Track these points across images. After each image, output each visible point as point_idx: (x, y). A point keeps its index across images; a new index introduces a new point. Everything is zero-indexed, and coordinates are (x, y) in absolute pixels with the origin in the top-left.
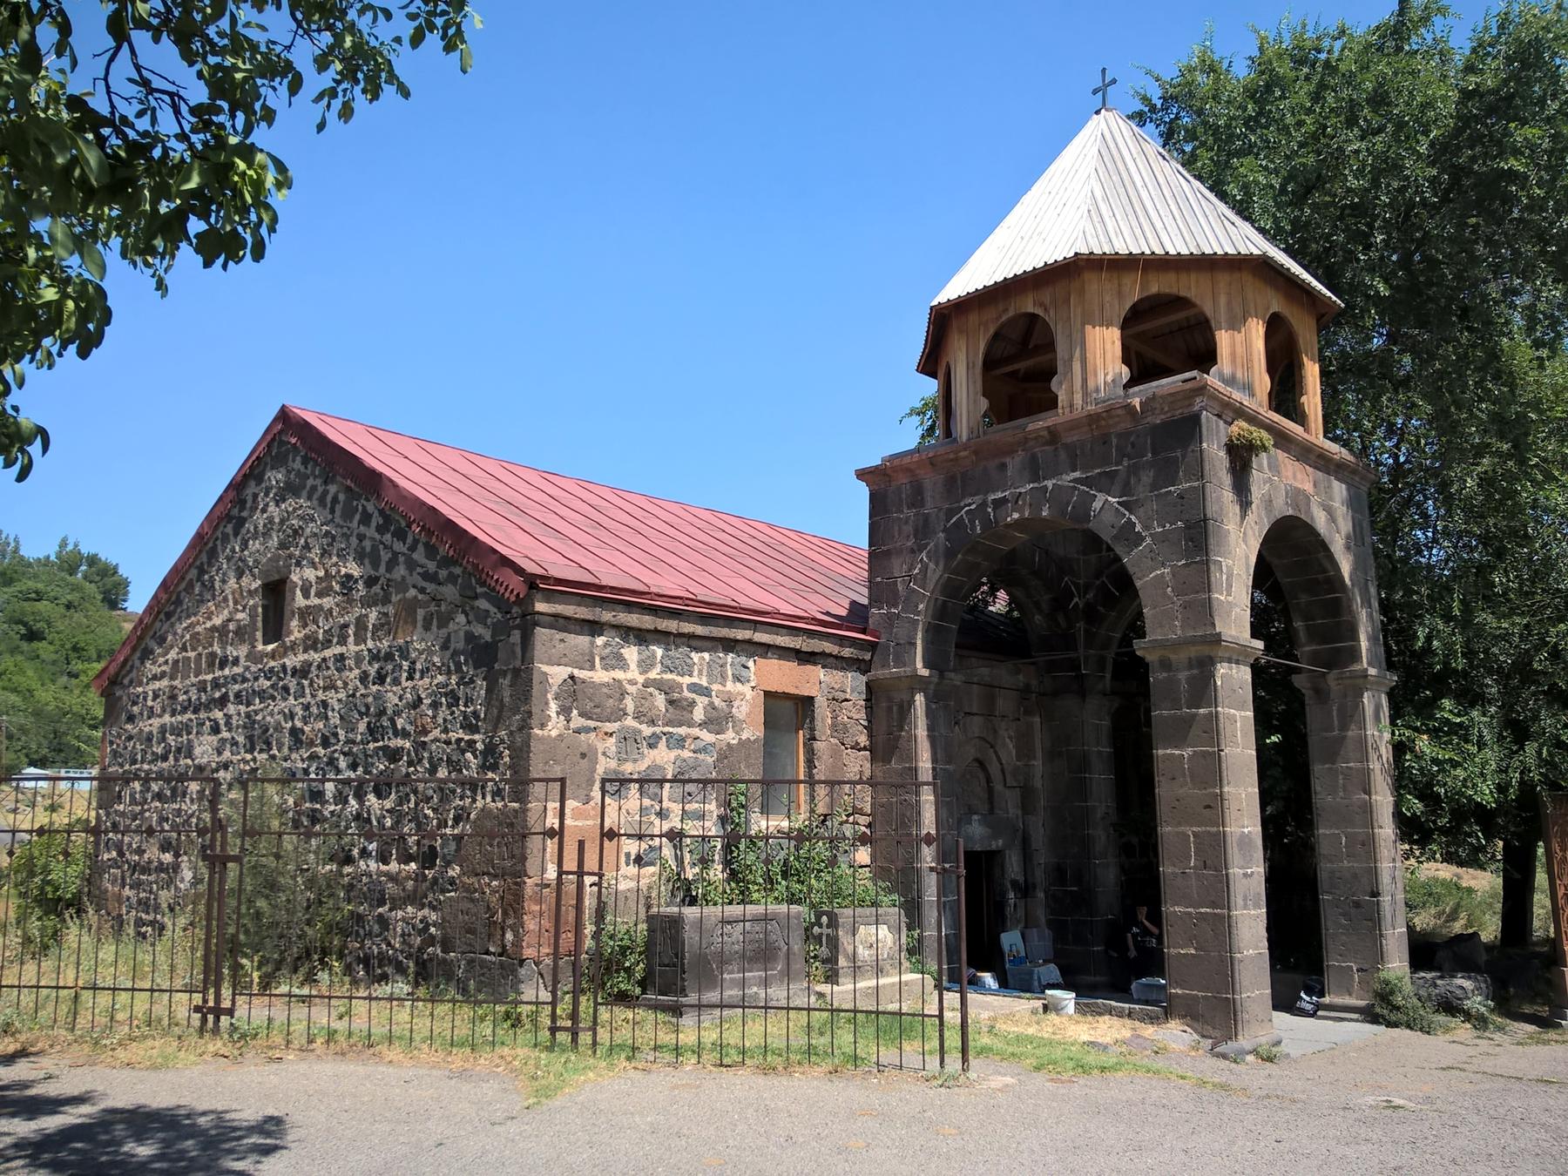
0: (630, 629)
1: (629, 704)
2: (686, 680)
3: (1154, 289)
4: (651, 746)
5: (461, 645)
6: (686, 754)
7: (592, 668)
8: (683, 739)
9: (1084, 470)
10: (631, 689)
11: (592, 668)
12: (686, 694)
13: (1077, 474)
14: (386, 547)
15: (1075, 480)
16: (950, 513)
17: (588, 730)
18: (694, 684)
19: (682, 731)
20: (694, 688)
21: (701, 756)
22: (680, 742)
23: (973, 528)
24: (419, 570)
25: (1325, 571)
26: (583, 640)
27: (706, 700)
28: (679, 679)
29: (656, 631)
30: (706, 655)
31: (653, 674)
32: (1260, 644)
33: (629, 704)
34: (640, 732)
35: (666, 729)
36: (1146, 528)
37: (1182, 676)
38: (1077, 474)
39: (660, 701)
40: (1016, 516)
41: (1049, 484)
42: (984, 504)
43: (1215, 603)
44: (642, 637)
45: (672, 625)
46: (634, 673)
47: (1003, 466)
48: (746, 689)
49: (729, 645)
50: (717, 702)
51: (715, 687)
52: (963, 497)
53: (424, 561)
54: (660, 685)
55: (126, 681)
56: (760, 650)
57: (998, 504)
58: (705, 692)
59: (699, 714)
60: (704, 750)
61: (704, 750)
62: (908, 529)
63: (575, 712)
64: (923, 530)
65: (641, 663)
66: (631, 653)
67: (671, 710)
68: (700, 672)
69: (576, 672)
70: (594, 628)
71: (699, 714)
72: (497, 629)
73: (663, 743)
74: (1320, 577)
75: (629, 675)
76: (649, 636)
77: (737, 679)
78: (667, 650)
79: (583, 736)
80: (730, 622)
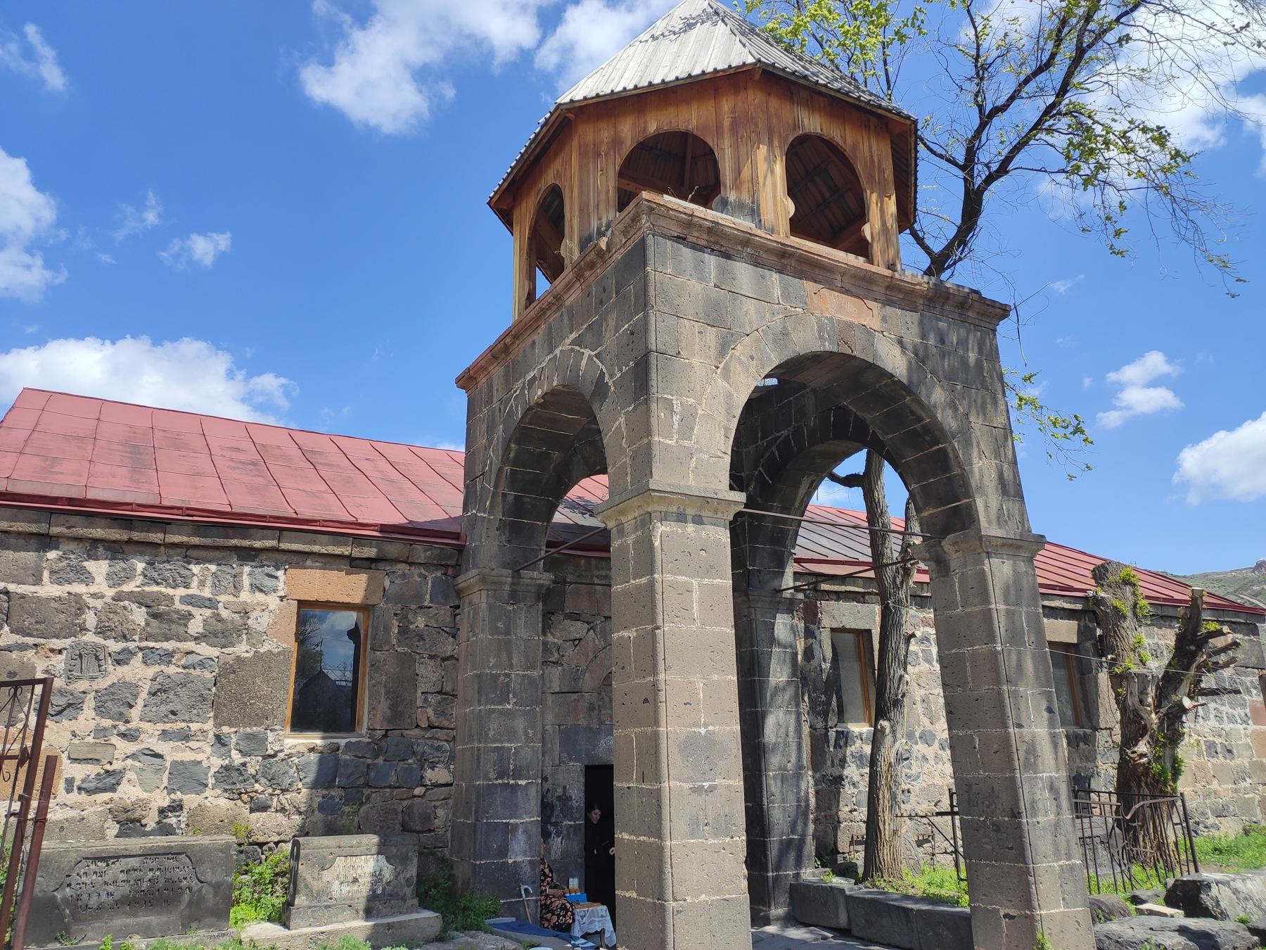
0: (95, 541)
1: (90, 619)
2: (181, 591)
3: (652, 128)
4: (119, 662)
6: (171, 670)
7: (38, 581)
8: (170, 654)
10: (92, 602)
11: (38, 581)
12: (178, 605)
13: (574, 335)
15: (574, 343)
17: (23, 647)
18: (192, 596)
19: (169, 645)
20: (190, 600)
21: (198, 672)
22: (167, 657)
25: (920, 419)
26: (28, 557)
27: (208, 612)
28: (170, 591)
29: (130, 542)
30: (213, 568)
31: (129, 587)
32: (741, 497)
33: (90, 619)
34: (104, 647)
35: (144, 644)
36: (611, 376)
37: (630, 540)
39: (139, 616)
40: (539, 392)
41: (557, 352)
42: (523, 388)
43: (656, 450)
44: (116, 550)
45: (157, 537)
46: (100, 585)
47: (534, 342)
48: (273, 601)
49: (248, 555)
50: (224, 614)
51: (223, 598)
54: (141, 600)
56: (294, 558)
58: (211, 604)
59: (195, 626)
60: (202, 665)
61: (202, 665)
62: (484, 427)
63: (6, 628)
64: (490, 430)
65: (109, 577)
66: (99, 568)
67: (155, 623)
68: (202, 584)
69: (12, 587)
70: (45, 542)
71: (195, 626)
73: (137, 660)
74: (918, 426)
75: (93, 589)
76: (126, 548)
77: (256, 588)
78: (151, 564)
79: (14, 655)
80: (243, 531)
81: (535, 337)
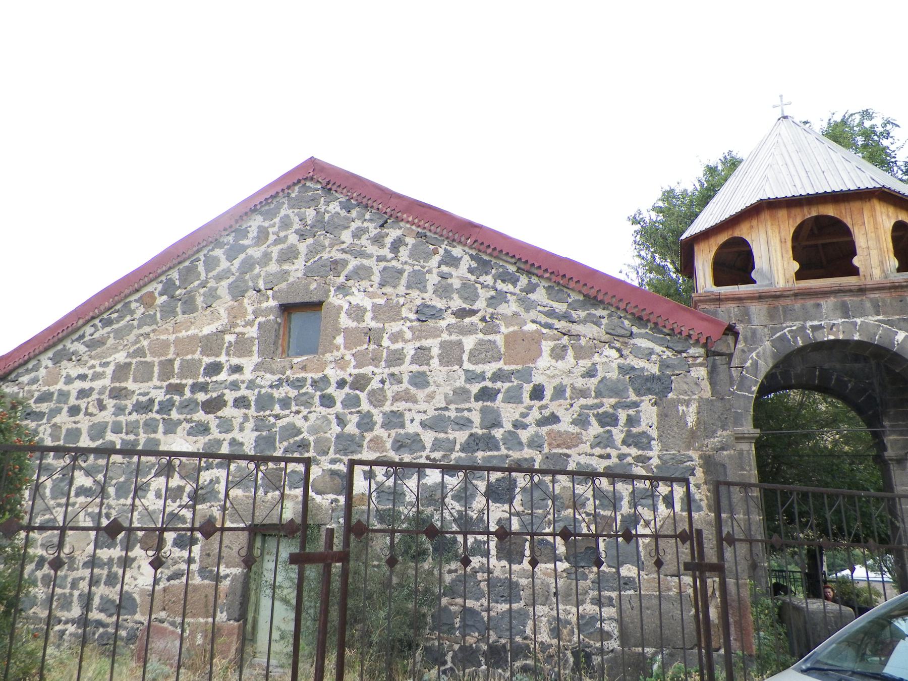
5: (614, 375)
9: (884, 314)
13: (880, 317)
14: (484, 286)
16: (774, 331)
23: (795, 341)
24: (539, 308)
38: (880, 317)
40: (832, 337)
42: (803, 328)
47: (819, 305)
52: (785, 321)
53: (546, 301)
55: (25, 379)
57: (815, 328)
72: (664, 365)
81: (822, 302)
